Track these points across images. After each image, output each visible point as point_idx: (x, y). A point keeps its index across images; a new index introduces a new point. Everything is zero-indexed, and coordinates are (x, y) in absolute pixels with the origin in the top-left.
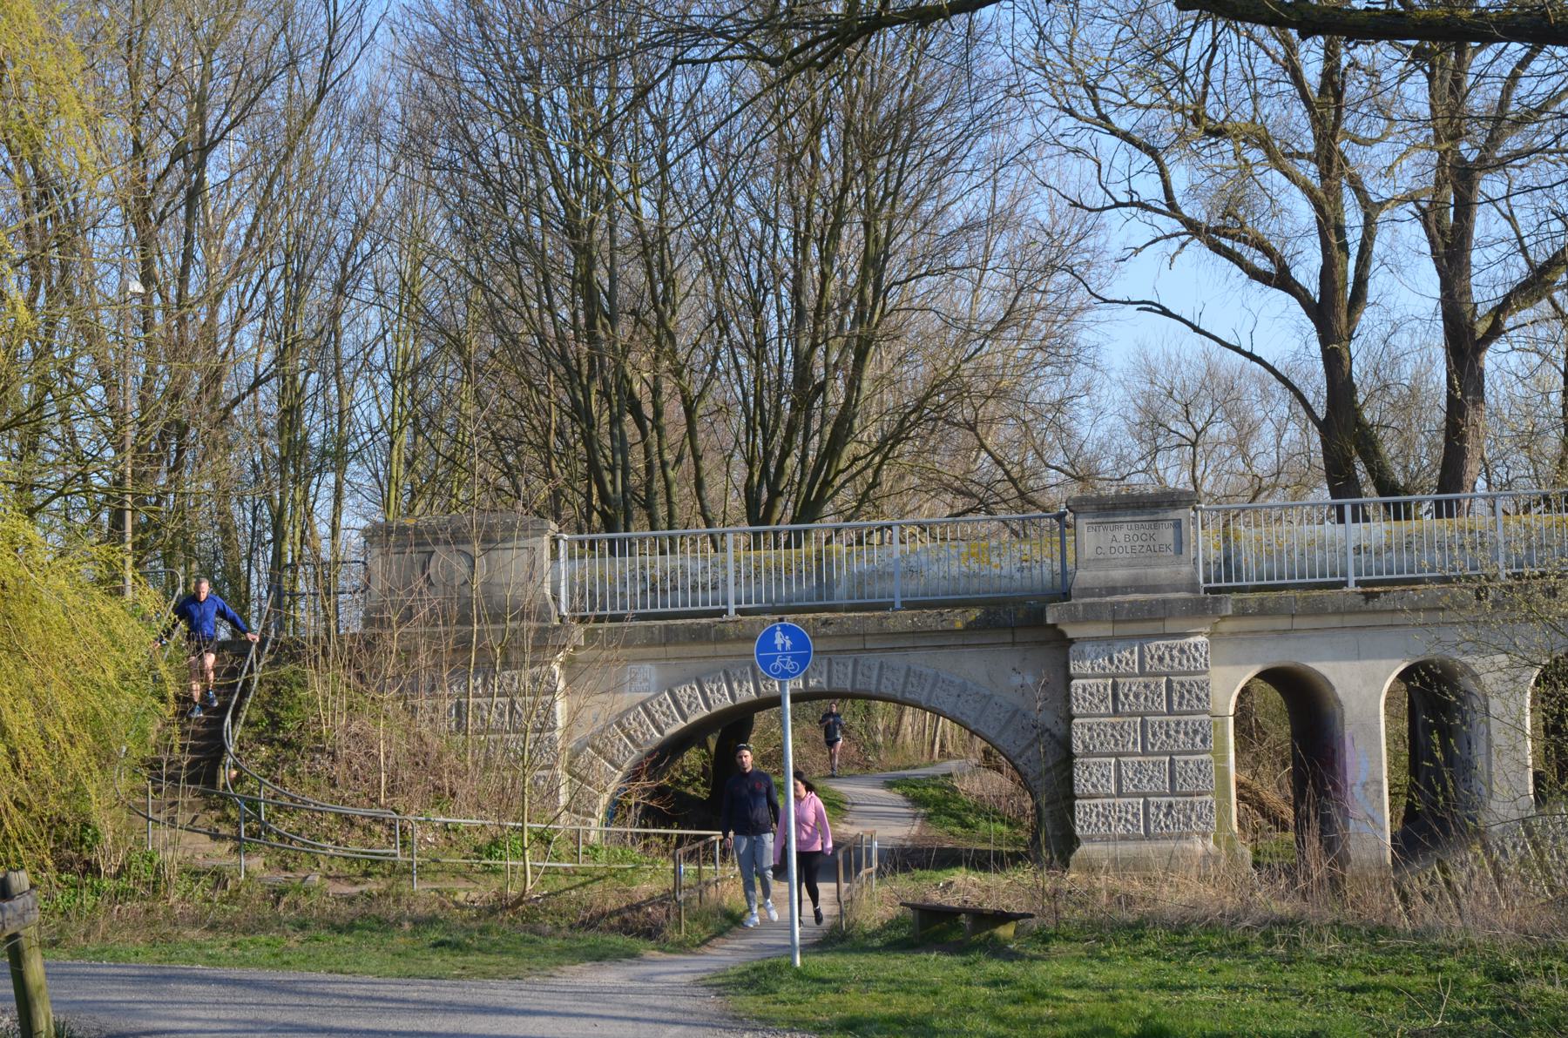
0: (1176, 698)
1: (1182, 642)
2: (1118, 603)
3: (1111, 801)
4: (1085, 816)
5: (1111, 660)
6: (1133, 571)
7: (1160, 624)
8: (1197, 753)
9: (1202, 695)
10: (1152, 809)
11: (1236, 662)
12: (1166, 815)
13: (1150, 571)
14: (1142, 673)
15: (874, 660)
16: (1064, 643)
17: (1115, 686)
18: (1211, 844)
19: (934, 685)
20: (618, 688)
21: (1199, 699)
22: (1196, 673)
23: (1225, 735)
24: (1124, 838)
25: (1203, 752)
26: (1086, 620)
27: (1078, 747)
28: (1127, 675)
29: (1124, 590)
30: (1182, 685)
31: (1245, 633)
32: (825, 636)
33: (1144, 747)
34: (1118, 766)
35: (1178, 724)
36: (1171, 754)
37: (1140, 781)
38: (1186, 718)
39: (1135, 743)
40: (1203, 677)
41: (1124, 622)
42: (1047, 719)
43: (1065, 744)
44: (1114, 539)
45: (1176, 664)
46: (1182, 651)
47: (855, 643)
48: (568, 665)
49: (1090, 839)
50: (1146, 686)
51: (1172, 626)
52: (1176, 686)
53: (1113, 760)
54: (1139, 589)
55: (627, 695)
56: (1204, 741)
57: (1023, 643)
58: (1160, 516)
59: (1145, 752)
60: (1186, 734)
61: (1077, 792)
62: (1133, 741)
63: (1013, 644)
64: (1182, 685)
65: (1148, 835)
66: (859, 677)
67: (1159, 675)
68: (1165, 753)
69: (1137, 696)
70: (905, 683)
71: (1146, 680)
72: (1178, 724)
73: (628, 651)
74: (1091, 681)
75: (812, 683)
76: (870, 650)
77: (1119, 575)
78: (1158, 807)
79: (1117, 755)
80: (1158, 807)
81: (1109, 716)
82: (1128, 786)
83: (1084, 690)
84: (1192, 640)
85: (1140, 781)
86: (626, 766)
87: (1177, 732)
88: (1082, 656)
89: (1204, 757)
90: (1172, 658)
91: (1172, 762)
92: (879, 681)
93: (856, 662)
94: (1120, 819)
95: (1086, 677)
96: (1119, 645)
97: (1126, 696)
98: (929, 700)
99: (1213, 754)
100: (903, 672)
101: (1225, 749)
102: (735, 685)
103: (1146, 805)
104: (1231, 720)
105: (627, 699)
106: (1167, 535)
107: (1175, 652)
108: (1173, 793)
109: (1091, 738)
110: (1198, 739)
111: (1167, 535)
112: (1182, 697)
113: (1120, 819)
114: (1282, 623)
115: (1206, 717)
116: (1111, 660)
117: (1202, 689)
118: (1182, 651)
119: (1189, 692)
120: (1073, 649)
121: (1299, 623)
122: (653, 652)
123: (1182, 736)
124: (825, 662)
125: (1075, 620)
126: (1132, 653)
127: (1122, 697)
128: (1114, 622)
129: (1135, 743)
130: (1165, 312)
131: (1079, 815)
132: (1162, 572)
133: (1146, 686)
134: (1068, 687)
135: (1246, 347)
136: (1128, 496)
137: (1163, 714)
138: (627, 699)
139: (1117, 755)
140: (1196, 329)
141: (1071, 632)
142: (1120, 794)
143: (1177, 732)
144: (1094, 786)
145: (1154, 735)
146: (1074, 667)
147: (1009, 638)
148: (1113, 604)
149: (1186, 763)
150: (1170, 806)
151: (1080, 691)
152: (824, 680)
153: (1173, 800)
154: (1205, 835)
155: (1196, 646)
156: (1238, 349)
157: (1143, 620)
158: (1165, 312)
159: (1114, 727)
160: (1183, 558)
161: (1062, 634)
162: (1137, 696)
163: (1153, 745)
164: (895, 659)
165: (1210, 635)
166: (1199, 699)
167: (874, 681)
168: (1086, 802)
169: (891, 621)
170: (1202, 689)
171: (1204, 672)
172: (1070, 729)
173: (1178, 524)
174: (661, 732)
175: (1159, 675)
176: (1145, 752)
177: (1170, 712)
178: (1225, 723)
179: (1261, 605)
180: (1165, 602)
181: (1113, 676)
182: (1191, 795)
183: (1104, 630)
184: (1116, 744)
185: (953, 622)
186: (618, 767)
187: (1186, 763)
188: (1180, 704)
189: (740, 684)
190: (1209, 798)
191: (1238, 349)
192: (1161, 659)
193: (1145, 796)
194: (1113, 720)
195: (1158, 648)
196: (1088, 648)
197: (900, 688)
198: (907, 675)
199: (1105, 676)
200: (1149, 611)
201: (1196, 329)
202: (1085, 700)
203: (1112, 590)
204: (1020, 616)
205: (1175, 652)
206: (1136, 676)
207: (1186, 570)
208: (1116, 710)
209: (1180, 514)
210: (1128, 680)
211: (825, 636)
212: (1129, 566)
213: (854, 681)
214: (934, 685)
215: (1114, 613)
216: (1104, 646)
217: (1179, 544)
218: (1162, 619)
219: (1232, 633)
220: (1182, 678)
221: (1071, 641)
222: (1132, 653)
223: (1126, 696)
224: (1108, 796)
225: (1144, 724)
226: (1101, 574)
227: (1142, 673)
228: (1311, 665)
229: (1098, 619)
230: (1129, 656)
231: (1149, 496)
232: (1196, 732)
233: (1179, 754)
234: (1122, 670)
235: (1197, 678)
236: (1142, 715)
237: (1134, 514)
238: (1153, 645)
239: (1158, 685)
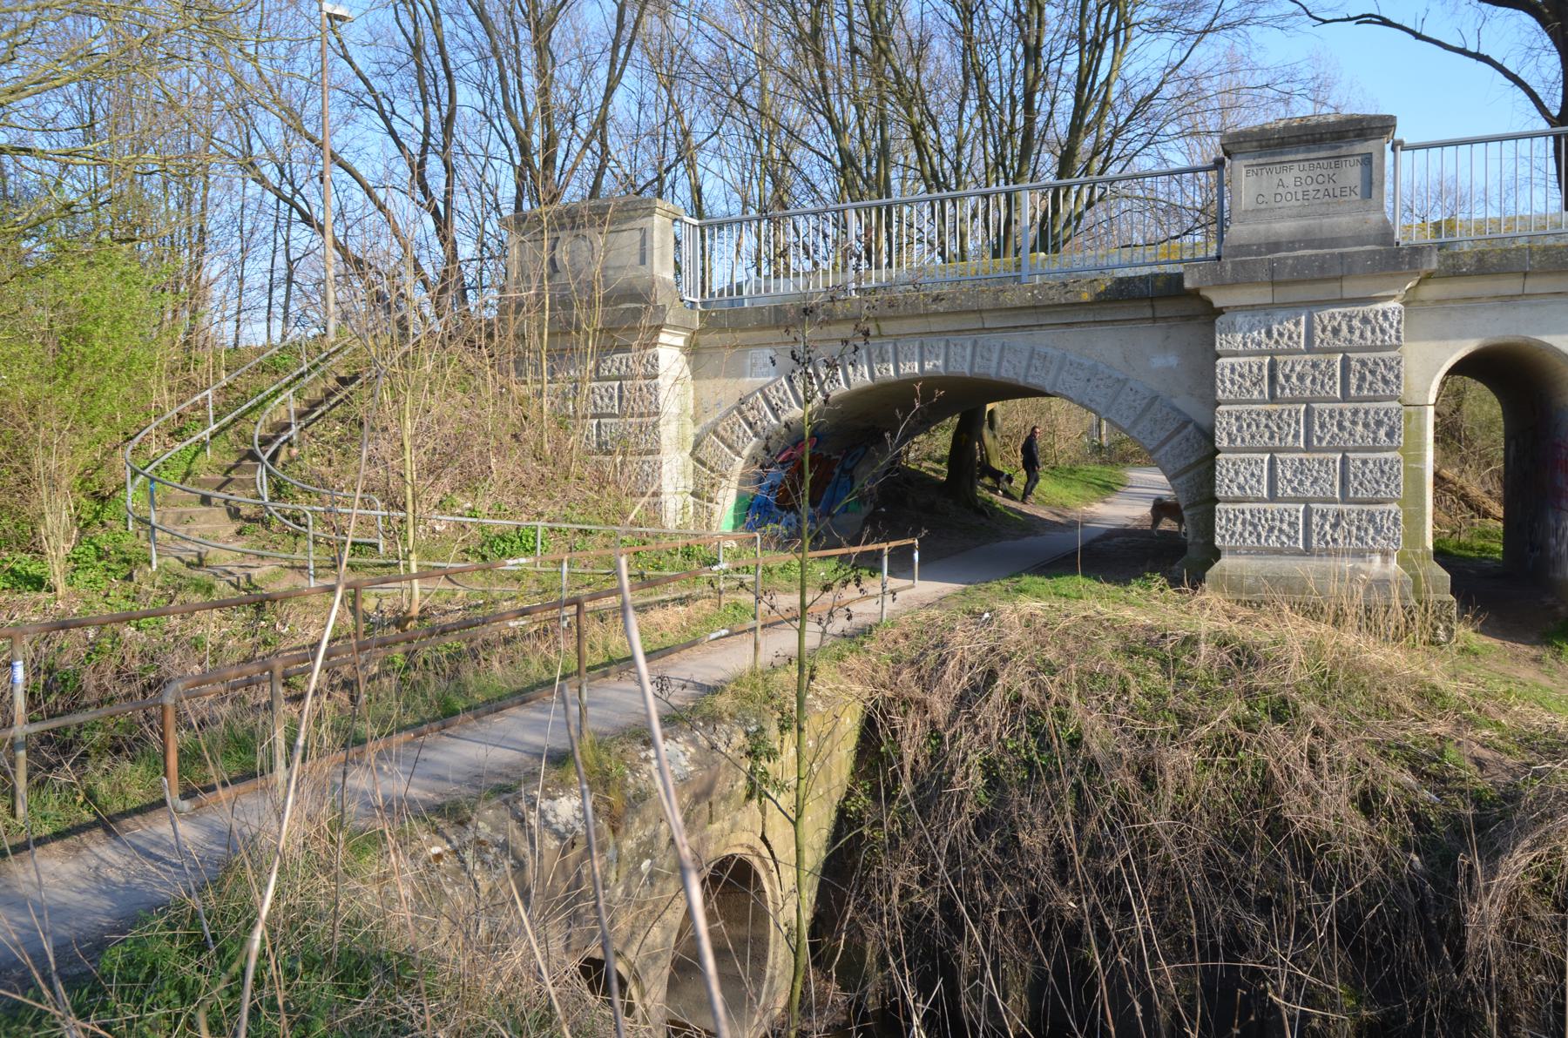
0: (1354, 381)
1: (1366, 309)
2: (1279, 259)
3: (1262, 506)
4: (1228, 524)
5: (1269, 334)
6: (1304, 222)
7: (1335, 286)
8: (1381, 450)
9: (1391, 376)
10: (1316, 519)
11: (1443, 337)
12: (1334, 526)
13: (1326, 221)
14: (1310, 348)
15: (995, 340)
16: (1210, 314)
17: (1273, 366)
18: (1394, 565)
19: (1060, 368)
20: (742, 375)
21: (1386, 381)
22: (1383, 348)
23: (1421, 429)
24: (1278, 552)
25: (1389, 449)
26: (1235, 284)
27: (1222, 441)
28: (1290, 352)
29: (1291, 245)
30: (1363, 363)
31: (1455, 300)
32: (936, 314)
33: (1308, 441)
34: (1272, 462)
35: (1355, 413)
36: (1344, 451)
37: (1301, 483)
38: (1366, 405)
39: (1296, 436)
40: (1393, 354)
41: (1286, 283)
42: (1189, 406)
43: (1208, 435)
44: (1281, 184)
45: (1356, 337)
46: (1365, 320)
47: (972, 322)
48: (693, 351)
49: (1234, 551)
50: (1315, 366)
51: (1351, 289)
52: (1355, 365)
53: (1267, 457)
54: (1309, 244)
55: (748, 379)
56: (1390, 435)
57: (1165, 319)
58: (1344, 151)
59: (1309, 447)
60: (1366, 425)
61: (1219, 493)
62: (1294, 434)
63: (1154, 319)
64: (1363, 363)
65: (1308, 551)
66: (978, 359)
67: (1333, 351)
68: (1336, 450)
69: (1301, 378)
70: (1029, 366)
71: (1314, 357)
72: (1355, 413)
73: (740, 336)
74: (1242, 360)
75: (928, 366)
76: (990, 330)
77: (1284, 227)
78: (1324, 516)
79: (1272, 451)
80: (1324, 516)
81: (1264, 402)
82: (1284, 489)
83: (1233, 370)
84: (1379, 306)
85: (1301, 483)
86: (746, 453)
87: (1354, 423)
88: (1232, 328)
89: (1389, 455)
90: (1351, 330)
91: (1344, 461)
92: (999, 364)
93: (975, 343)
94: (1271, 529)
95: (1236, 354)
96: (1280, 314)
97: (1288, 378)
98: (1054, 385)
99: (1403, 451)
100: (1027, 354)
101: (1420, 446)
102: (850, 369)
103: (1308, 514)
104: (1431, 411)
105: (749, 383)
106: (1352, 174)
107: (1356, 323)
108: (1345, 499)
109: (1240, 429)
110: (1382, 433)
111: (1352, 174)
112: (1362, 378)
113: (1271, 529)
114: (1510, 285)
115: (1395, 404)
116: (1269, 334)
117: (1391, 369)
118: (1365, 320)
119: (1372, 372)
120: (1220, 321)
121: (1534, 285)
122: (769, 335)
123: (1360, 428)
124: (942, 344)
125: (1222, 284)
126: (1297, 324)
127: (1281, 379)
128: (1273, 283)
129: (1296, 436)
130: (1386, 22)
131: (1220, 522)
132: (1344, 221)
133: (1315, 366)
134: (1215, 366)
135: (1472, 48)
136: (1300, 127)
137: (1335, 401)
138: (749, 383)
139: (1272, 451)
140: (1418, 36)
141: (1219, 299)
142: (1273, 497)
143: (1354, 423)
144: (1240, 487)
145: (1322, 426)
146: (1221, 342)
147: (1148, 313)
148: (1271, 261)
149: (1365, 462)
150: (1339, 516)
151: (1227, 372)
152: (940, 363)
153: (1345, 508)
154: (1385, 554)
155: (1385, 314)
156: (1463, 52)
157: (1313, 281)
158: (1386, 22)
159: (1269, 416)
160: (1373, 202)
161: (1210, 303)
162: (1301, 378)
163: (1320, 439)
164: (1019, 340)
165: (1405, 304)
166: (1386, 381)
167: (994, 364)
168: (1229, 506)
169: (1008, 295)
170: (1391, 369)
171: (1395, 348)
172: (1214, 418)
173: (1367, 160)
174: (777, 418)
175: (1333, 351)
176: (1309, 447)
177: (1346, 397)
178: (1421, 415)
179: (1480, 260)
180: (1342, 255)
181: (1272, 353)
182: (1369, 502)
183: (1261, 295)
184: (1272, 437)
185: (1079, 293)
186: (739, 454)
187: (1365, 462)
188: (1359, 388)
189: (855, 370)
190: (1394, 507)
191: (1463, 52)
192: (1336, 331)
193: (1307, 501)
194: (1269, 407)
195: (1332, 317)
196: (1240, 319)
197: (1022, 372)
198: (1031, 357)
199: (1261, 353)
200: (1321, 268)
201: (1418, 36)
202: (1232, 382)
203: (1275, 246)
204: (1159, 284)
205: (1356, 323)
206: (1301, 352)
207: (1374, 217)
208: (1273, 398)
209: (1369, 146)
210: (1290, 359)
211: (936, 314)
212: (1300, 216)
213: (972, 364)
214: (1060, 368)
215: (1273, 271)
216: (1261, 316)
217: (1370, 185)
218: (1340, 278)
219: (1438, 301)
220: (1364, 356)
221: (1220, 312)
222: (1297, 324)
223: (1288, 378)
224: (1259, 500)
225: (1308, 413)
226: (1262, 227)
227: (1310, 348)
228: (1547, 339)
229: (1252, 282)
230: (1293, 329)
231: (1328, 124)
232: (1379, 423)
233: (1355, 450)
234: (1283, 345)
235: (1385, 355)
236: (1308, 402)
237: (1309, 151)
238: (1325, 314)
239: (1330, 364)
